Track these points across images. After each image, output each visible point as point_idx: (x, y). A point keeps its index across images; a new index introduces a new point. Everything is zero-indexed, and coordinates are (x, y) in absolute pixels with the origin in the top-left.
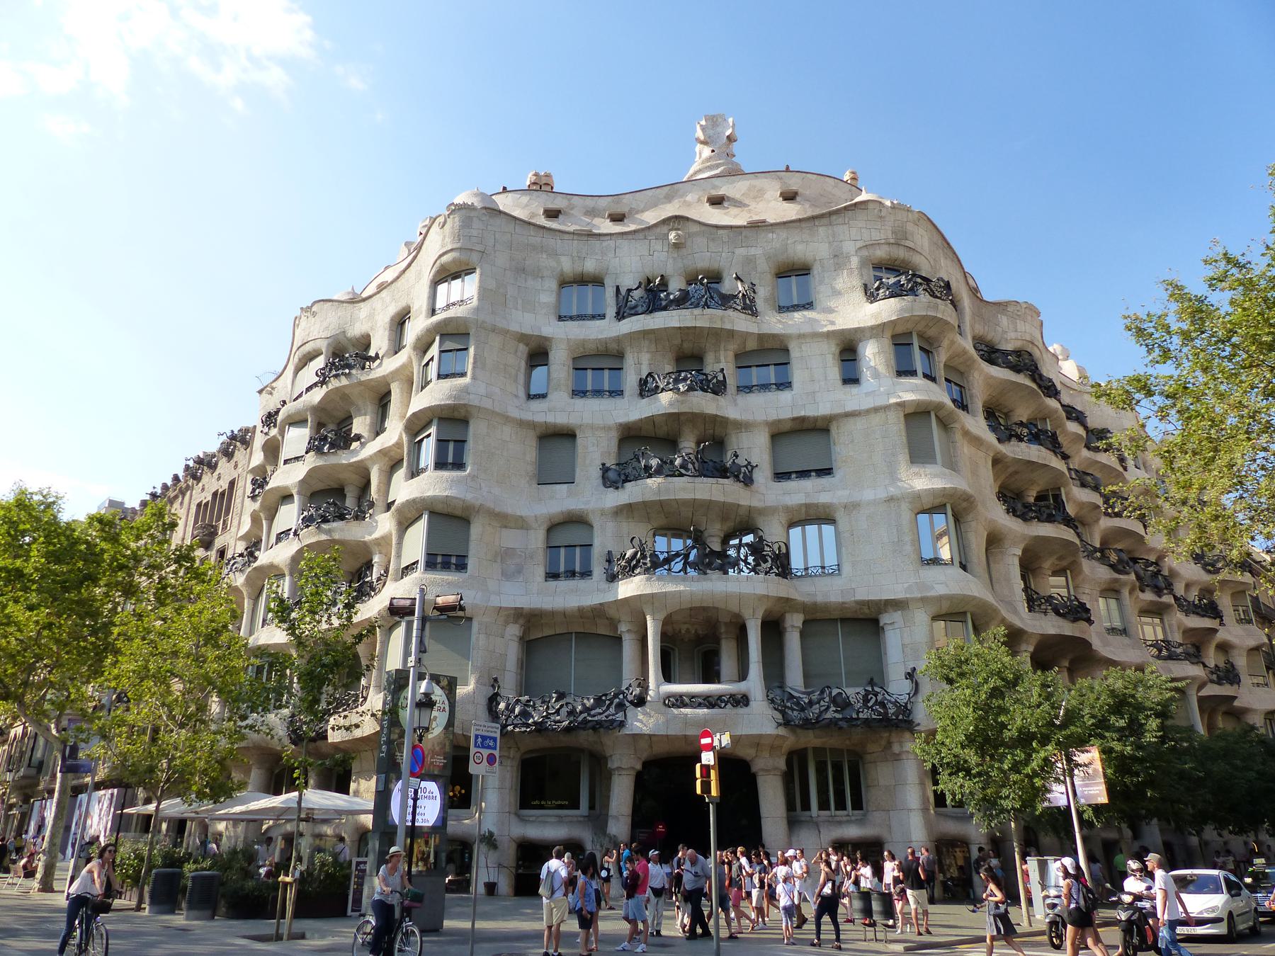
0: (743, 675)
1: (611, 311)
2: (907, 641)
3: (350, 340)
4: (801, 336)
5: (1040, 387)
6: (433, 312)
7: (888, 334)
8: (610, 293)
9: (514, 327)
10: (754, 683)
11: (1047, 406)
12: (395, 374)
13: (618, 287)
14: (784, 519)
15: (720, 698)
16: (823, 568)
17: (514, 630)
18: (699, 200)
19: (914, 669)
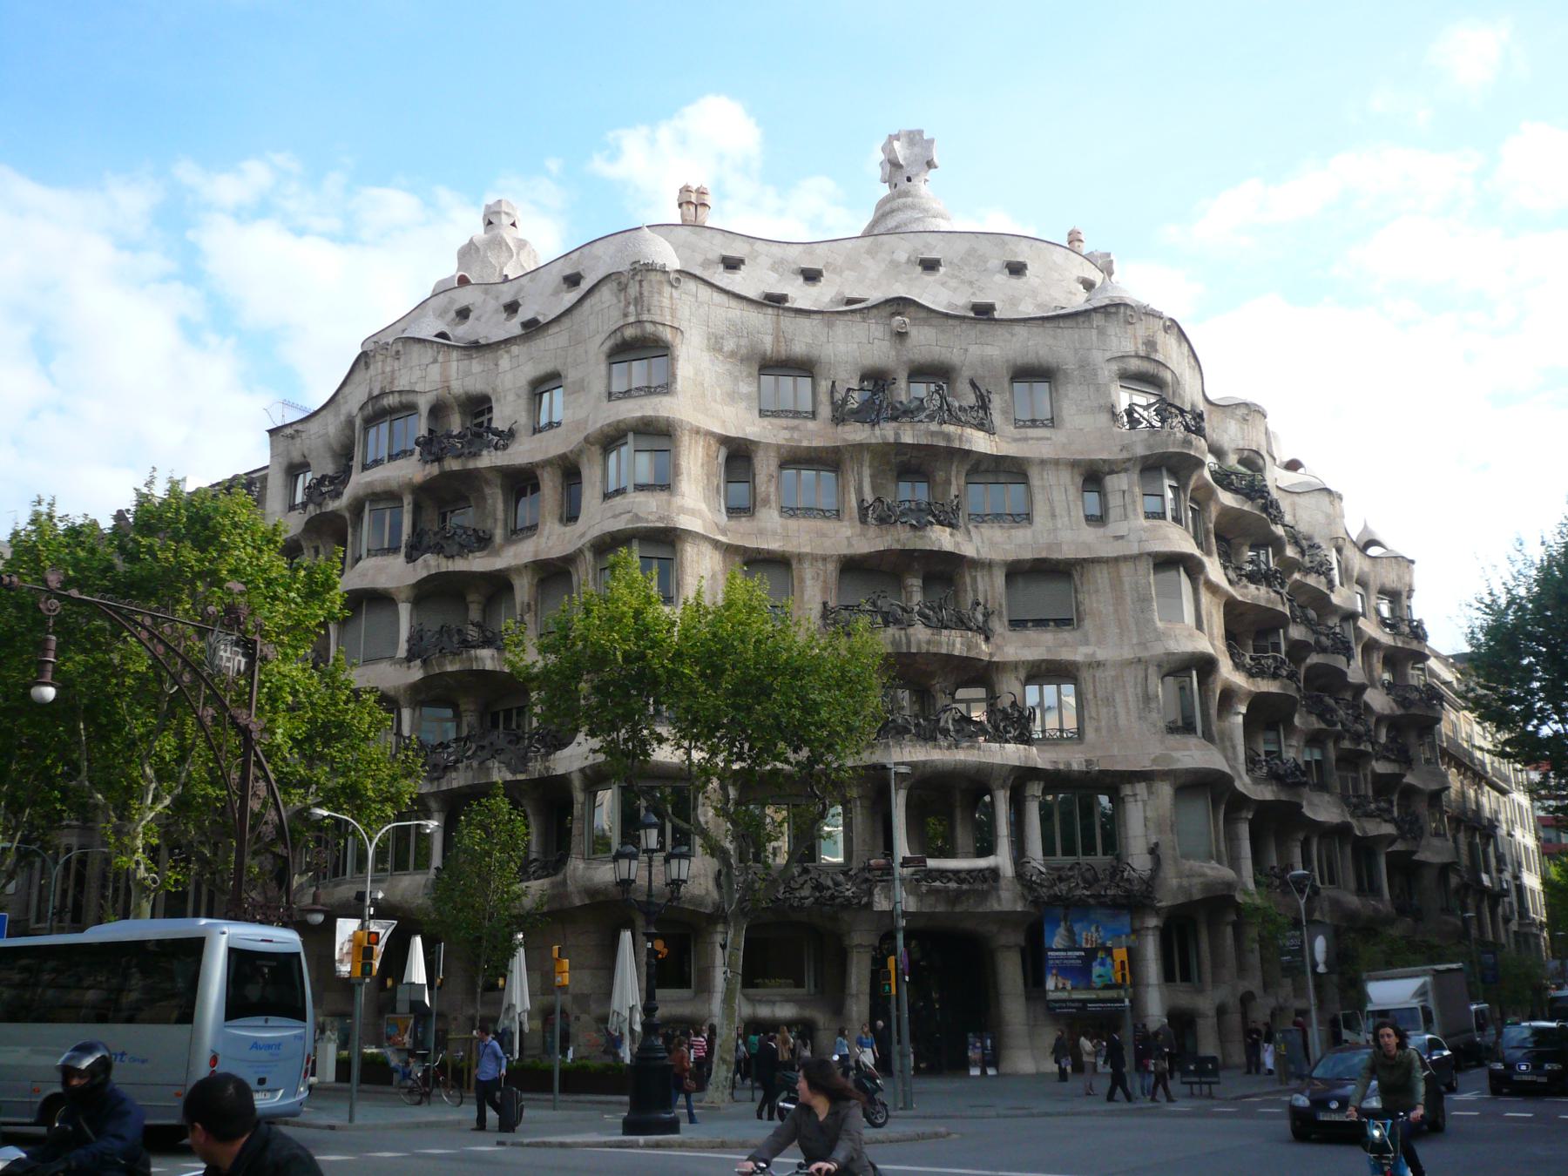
0: (986, 847)
1: (825, 411)
2: (1149, 814)
3: (456, 398)
4: (1043, 462)
5: (1269, 514)
6: (610, 394)
7: (1137, 471)
8: (824, 386)
9: (718, 429)
10: (1002, 858)
11: (1272, 533)
14: (1022, 675)
15: (969, 872)
16: (1061, 730)
18: (909, 260)
19: (1157, 844)
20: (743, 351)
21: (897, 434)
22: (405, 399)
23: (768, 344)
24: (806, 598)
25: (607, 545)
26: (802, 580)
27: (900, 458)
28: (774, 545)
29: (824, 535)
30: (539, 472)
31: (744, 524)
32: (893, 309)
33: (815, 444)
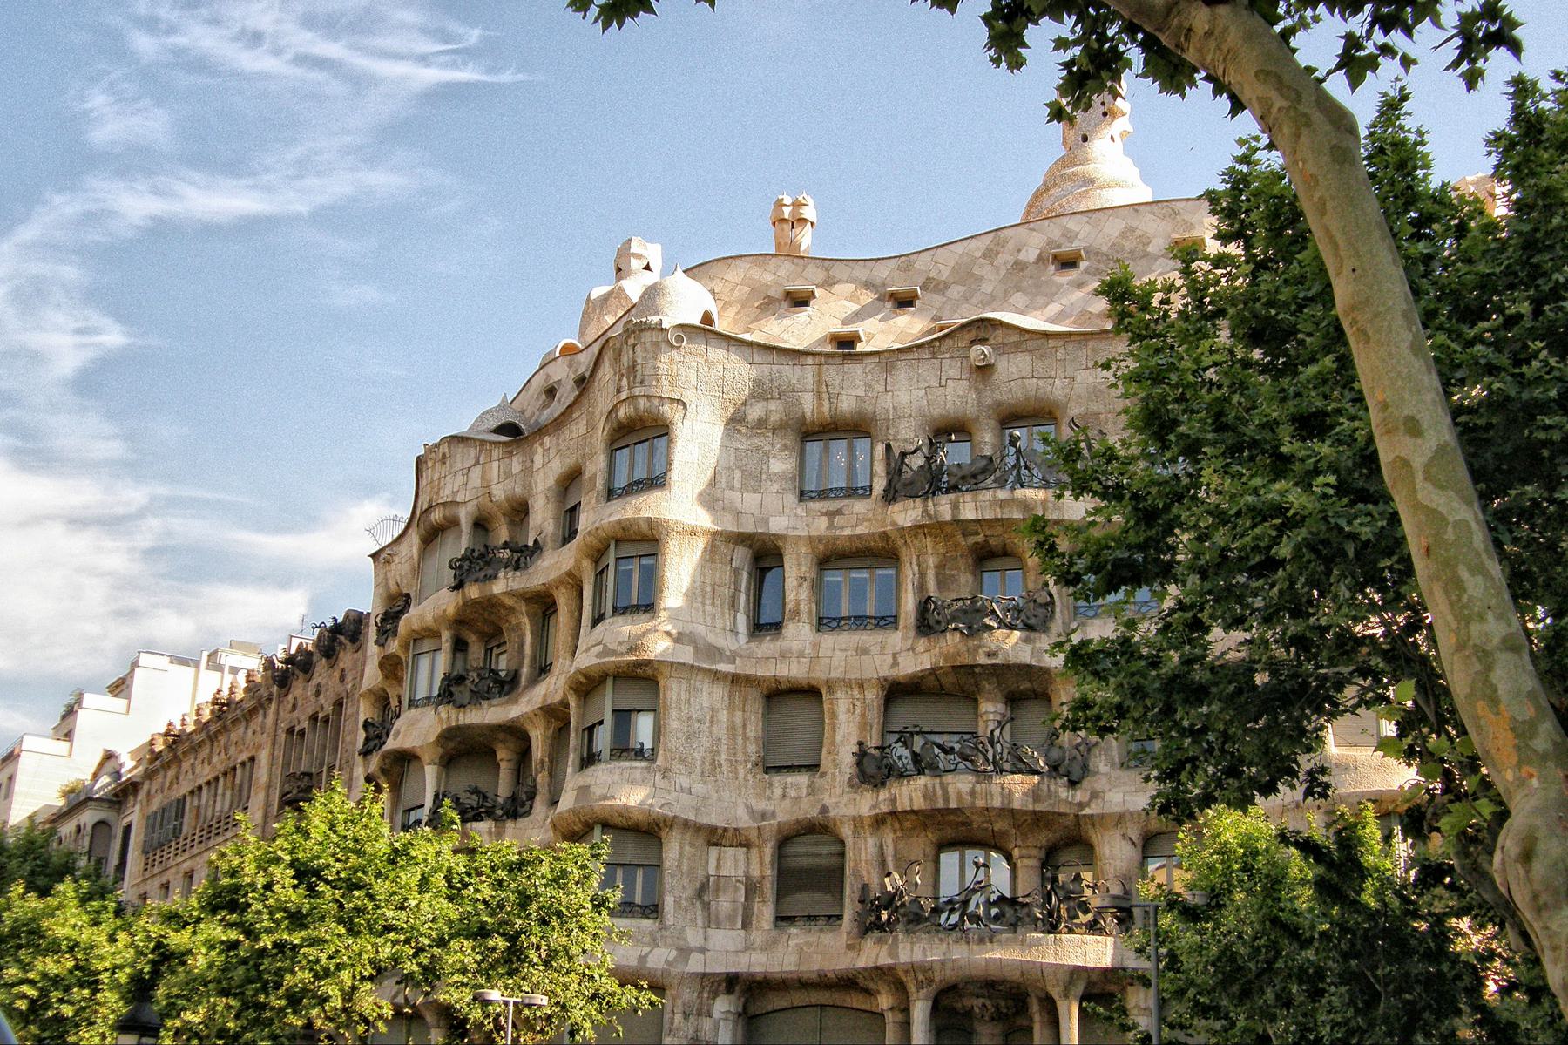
1: (880, 485)
8: (880, 448)
12: (560, 582)
13: (888, 447)
17: (723, 1005)
18: (1040, 259)
20: (774, 418)
21: (955, 507)
22: (448, 512)
23: (807, 404)
24: (838, 738)
25: (588, 686)
26: (834, 715)
27: (972, 540)
28: (793, 671)
29: (863, 651)
30: (555, 593)
31: (767, 646)
32: (973, 334)
33: (860, 530)
